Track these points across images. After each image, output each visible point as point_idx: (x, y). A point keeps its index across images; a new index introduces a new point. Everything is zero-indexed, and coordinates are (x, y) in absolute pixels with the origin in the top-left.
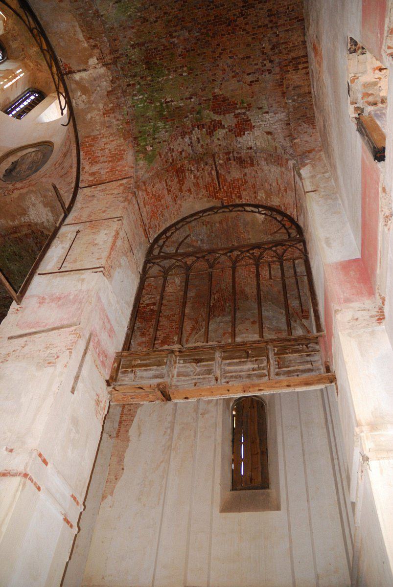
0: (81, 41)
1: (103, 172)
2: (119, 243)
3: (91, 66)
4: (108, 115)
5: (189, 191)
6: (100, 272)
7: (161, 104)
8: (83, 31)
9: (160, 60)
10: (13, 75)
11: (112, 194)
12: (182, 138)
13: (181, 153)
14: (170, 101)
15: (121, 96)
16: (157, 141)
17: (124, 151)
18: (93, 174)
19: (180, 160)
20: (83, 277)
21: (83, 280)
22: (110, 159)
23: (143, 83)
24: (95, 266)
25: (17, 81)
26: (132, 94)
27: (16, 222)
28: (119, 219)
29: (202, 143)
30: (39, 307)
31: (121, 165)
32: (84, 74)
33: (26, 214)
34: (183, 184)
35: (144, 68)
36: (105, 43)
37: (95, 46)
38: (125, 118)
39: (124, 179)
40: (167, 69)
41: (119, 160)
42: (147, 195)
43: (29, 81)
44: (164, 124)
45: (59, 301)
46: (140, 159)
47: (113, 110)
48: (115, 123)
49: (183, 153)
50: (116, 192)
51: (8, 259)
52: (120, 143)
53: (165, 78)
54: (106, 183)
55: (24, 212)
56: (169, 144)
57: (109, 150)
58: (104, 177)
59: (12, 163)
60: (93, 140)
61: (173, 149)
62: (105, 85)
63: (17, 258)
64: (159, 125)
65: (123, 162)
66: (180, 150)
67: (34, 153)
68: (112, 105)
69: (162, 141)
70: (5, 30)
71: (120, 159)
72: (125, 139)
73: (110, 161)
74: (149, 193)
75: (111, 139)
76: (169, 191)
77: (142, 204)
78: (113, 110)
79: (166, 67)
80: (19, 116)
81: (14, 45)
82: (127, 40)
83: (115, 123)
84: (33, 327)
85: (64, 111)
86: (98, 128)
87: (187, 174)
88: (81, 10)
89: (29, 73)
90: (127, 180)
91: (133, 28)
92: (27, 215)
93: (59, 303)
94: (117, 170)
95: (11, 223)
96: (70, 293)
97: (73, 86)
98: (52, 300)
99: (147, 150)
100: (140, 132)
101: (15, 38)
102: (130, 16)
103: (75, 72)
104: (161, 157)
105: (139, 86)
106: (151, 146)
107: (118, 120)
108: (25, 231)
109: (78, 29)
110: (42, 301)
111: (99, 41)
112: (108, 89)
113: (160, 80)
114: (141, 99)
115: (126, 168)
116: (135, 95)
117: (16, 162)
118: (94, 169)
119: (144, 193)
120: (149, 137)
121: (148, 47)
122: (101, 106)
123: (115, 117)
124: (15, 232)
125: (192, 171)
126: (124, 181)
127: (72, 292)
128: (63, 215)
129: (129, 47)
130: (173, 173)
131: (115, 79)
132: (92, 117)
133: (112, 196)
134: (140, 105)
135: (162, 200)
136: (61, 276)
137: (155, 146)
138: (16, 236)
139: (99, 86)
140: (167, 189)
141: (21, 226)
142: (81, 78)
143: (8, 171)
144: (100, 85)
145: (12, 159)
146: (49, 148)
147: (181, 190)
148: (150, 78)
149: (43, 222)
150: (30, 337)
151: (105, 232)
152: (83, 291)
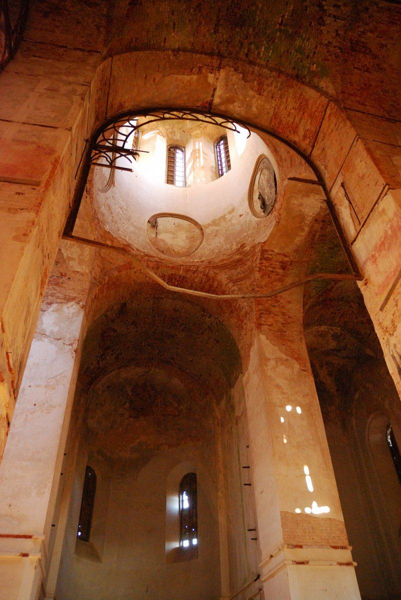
0: (191, 79)
1: (308, 127)
2: (378, 153)
3: (214, 82)
4: (262, 91)
5: (382, 46)
6: (387, 191)
7: (280, 30)
8: (183, 74)
9: (240, 8)
10: (197, 151)
11: (332, 131)
12: (324, 25)
13: (338, 35)
14: (282, 19)
15: (253, 68)
16: (311, 55)
17: (301, 94)
18: (305, 136)
19: (344, 40)
20: (380, 209)
21: (383, 211)
22: (302, 113)
23: (252, 40)
24: (380, 192)
25: (203, 152)
26: (256, 56)
27: (307, 229)
28: (356, 139)
29: (341, 4)
30: (377, 265)
31: (313, 105)
32: (218, 93)
33: (304, 217)
34: (371, 51)
35: (240, 30)
36: (202, 57)
37: (200, 68)
38: (274, 76)
39: (326, 110)
40: (252, 6)
41: (307, 105)
42: (356, 96)
43: (208, 142)
44: (300, 38)
45: (384, 246)
46: (318, 82)
47: (261, 84)
48: (273, 88)
49: (340, 32)
50: (332, 126)
51: (331, 257)
52: (293, 95)
53: (258, 13)
54: (319, 130)
55: (302, 217)
56: (321, 44)
57: (293, 108)
58: (313, 129)
59: (259, 198)
60: (276, 118)
61: (329, 42)
62: (236, 78)
63: (335, 249)
64: (298, 44)
65: (311, 102)
66: (334, 34)
67: (262, 176)
68: (256, 82)
69: (314, 50)
70: (164, 137)
71: (307, 103)
72: (293, 87)
73: (303, 114)
74: (354, 93)
75: (285, 101)
76: (367, 70)
77: (361, 108)
78: (261, 84)
79: (248, 6)
80: (229, 167)
81: (178, 136)
82: (207, 35)
83: (273, 88)
84: (388, 284)
85: (237, 130)
86: (269, 107)
87: (363, 40)
88: (168, 66)
89: (202, 137)
90: (329, 108)
91: (200, 23)
92: (306, 217)
93: (386, 246)
94: (315, 112)
95: (304, 234)
96: (386, 231)
97: (223, 108)
98: (380, 251)
99: (314, 71)
100: (294, 68)
101: (173, 133)
102: (190, 20)
103: (213, 100)
104: (329, 60)
105: (253, 45)
106: (313, 65)
107: (272, 84)
108: (317, 226)
109: (180, 77)
110: (374, 259)
111: (198, 63)
112: (240, 77)
113: (257, 20)
114: (265, 49)
115: (318, 103)
116: (259, 53)
117: (260, 195)
118: (301, 132)
119: (353, 98)
120: (304, 62)
121: (222, 16)
122: (251, 93)
123: (268, 85)
124: (314, 236)
125: (364, 33)
126: (328, 112)
127: (385, 228)
128: (321, 188)
129: (215, 36)
130: (352, 55)
131: (235, 67)
132: (257, 107)
133: (334, 132)
134: (270, 54)
135: (371, 83)
136: (367, 227)
137: (315, 60)
138: (317, 237)
139: (234, 85)
140: (364, 71)
141: (312, 227)
142: (220, 97)
143: (262, 207)
144: (233, 83)
145: (256, 196)
146: (265, 160)
147: (375, 57)
148: (251, 30)
149: (321, 207)
150: (394, 293)
151: (359, 160)
152: (393, 219)
